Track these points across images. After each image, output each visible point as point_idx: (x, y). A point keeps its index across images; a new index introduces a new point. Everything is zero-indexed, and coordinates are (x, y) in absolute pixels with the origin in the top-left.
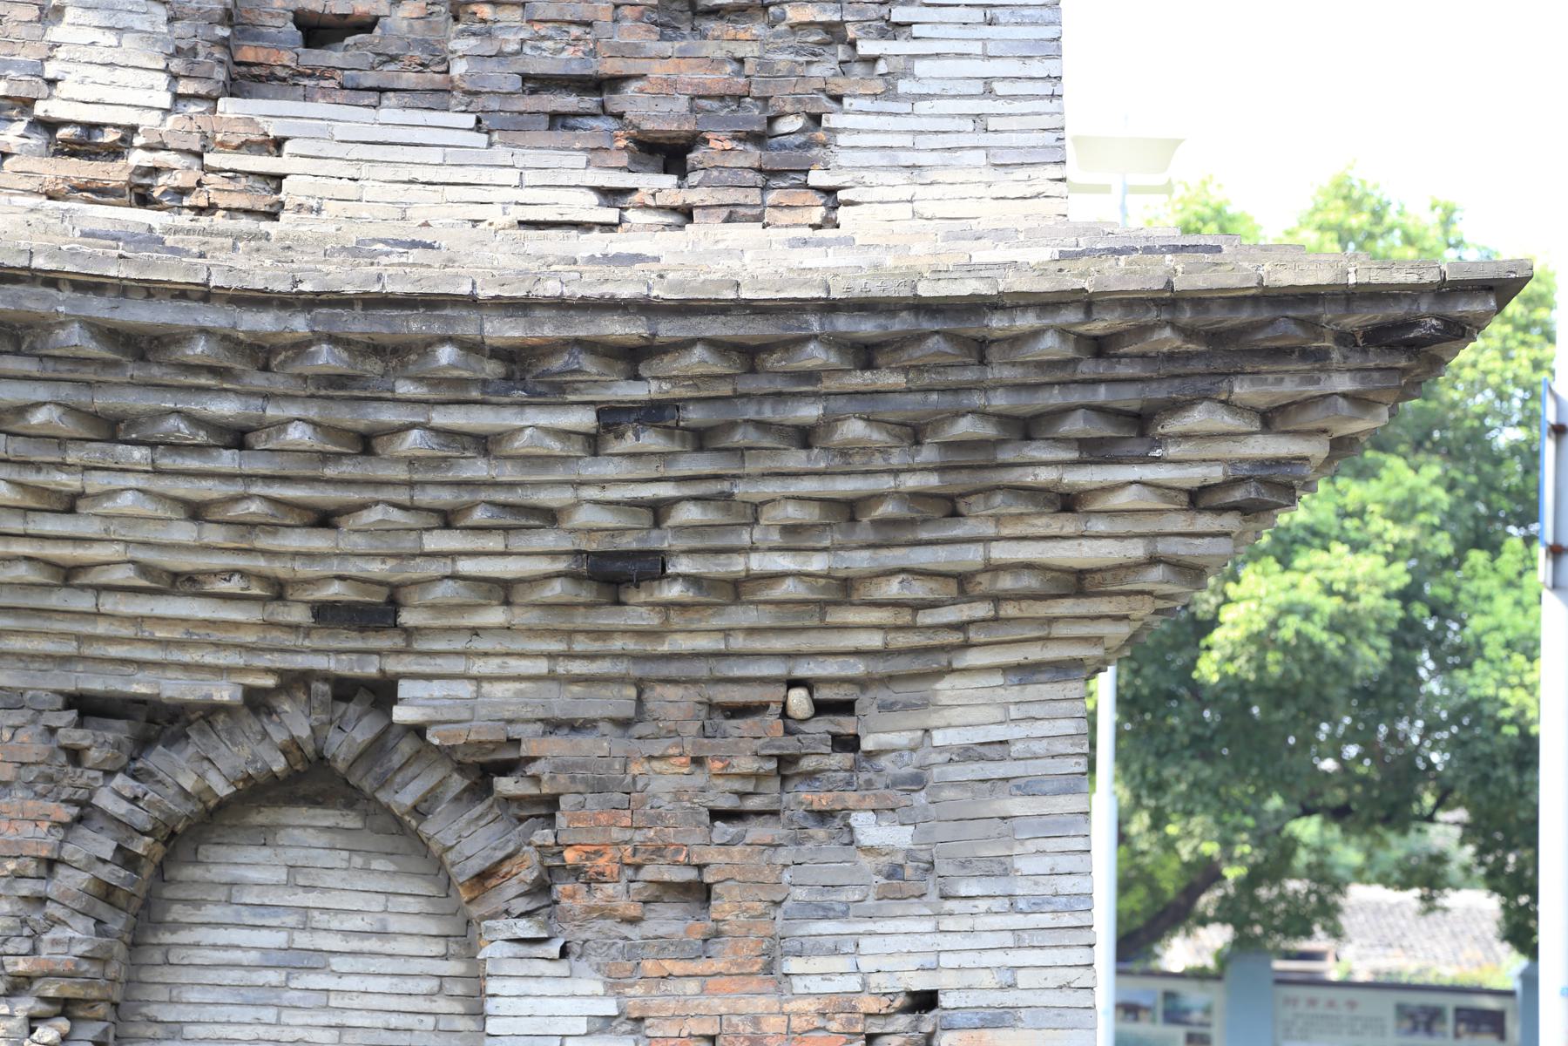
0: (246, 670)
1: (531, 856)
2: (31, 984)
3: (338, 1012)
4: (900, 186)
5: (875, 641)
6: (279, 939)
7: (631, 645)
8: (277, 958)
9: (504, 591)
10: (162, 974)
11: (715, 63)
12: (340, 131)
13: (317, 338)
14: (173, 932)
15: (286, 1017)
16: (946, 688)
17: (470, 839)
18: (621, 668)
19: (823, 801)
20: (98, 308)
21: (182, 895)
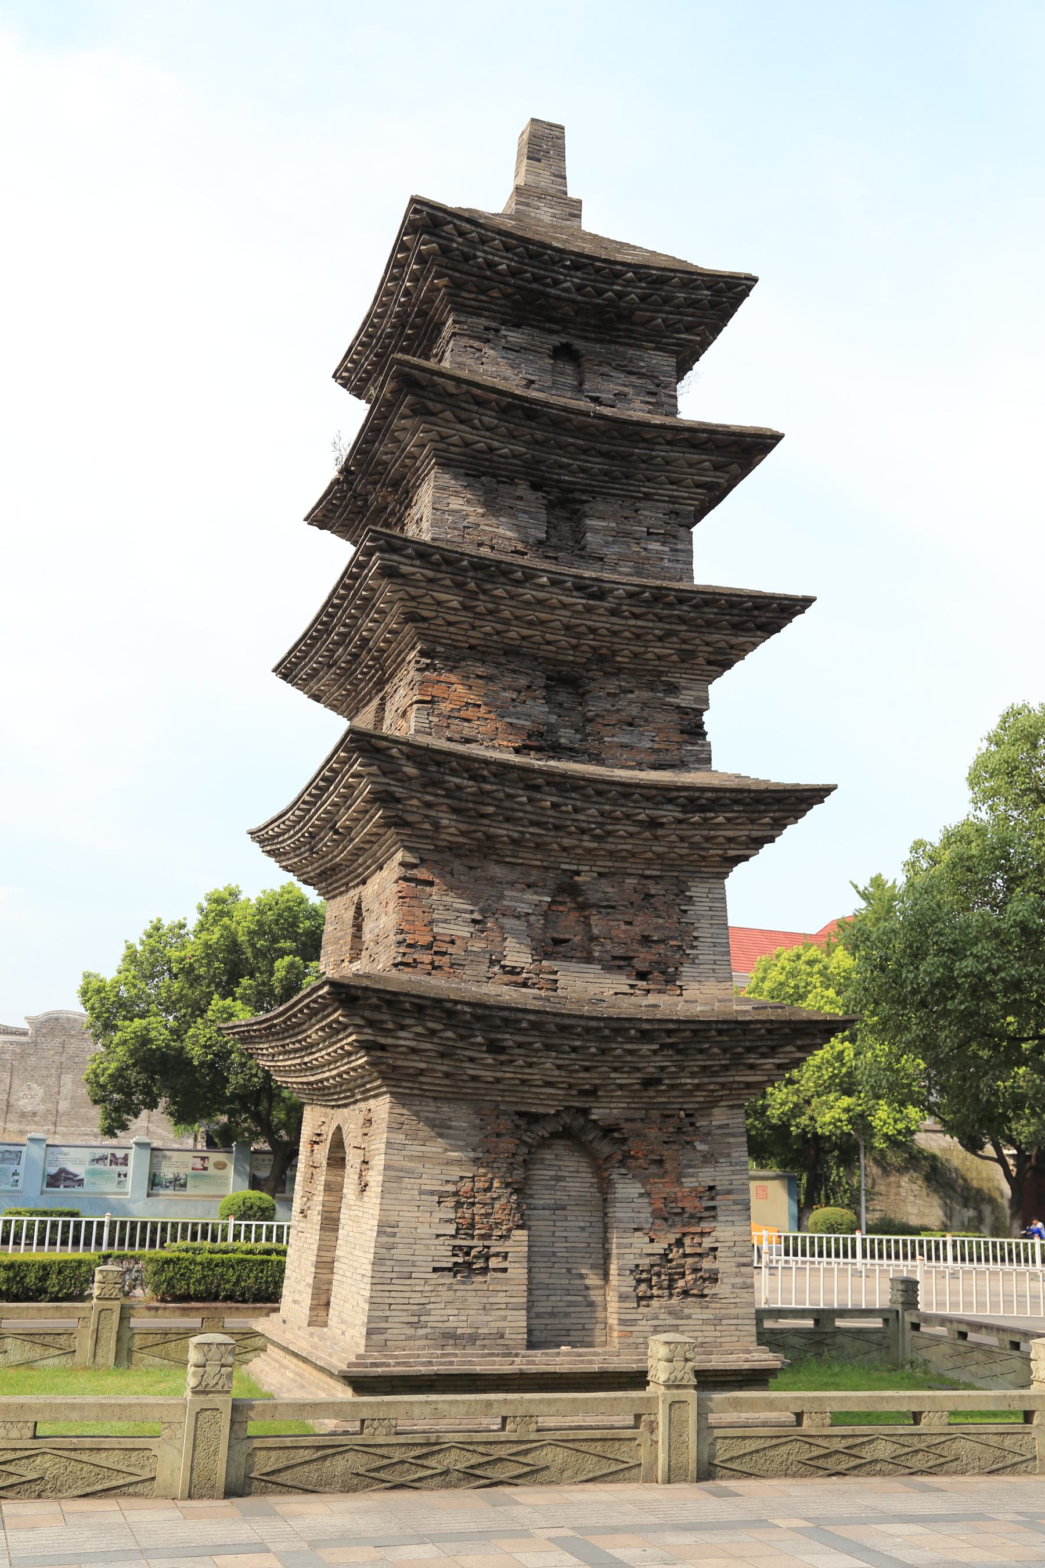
4: (696, 985)
5: (702, 1099)
6: (553, 1173)
9: (621, 1087)
11: (655, 954)
12: (571, 969)
13: (605, 1027)
16: (715, 1111)
17: (605, 1148)
18: (644, 1106)
19: (688, 1139)
20: (558, 1020)
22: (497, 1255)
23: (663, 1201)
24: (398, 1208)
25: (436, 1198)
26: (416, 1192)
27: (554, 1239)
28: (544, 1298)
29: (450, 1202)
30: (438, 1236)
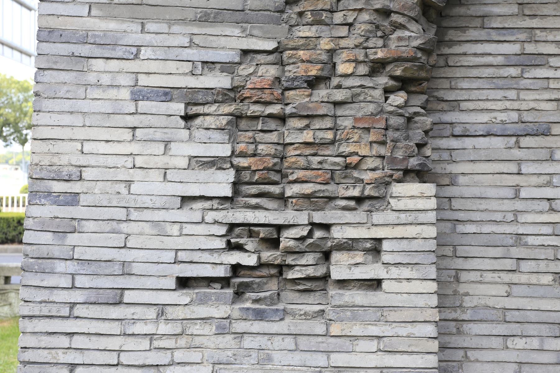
2: (384, 68)
3: (555, 91)
6: (515, 48)
8: (514, 60)
10: (444, 73)
14: (450, 47)
15: (523, 95)
21: (454, 24)
22: (348, 246)
24: (81, 134)
25: (179, 108)
26: (125, 94)
27: (519, 205)
28: (496, 342)
29: (216, 115)
30: (186, 200)
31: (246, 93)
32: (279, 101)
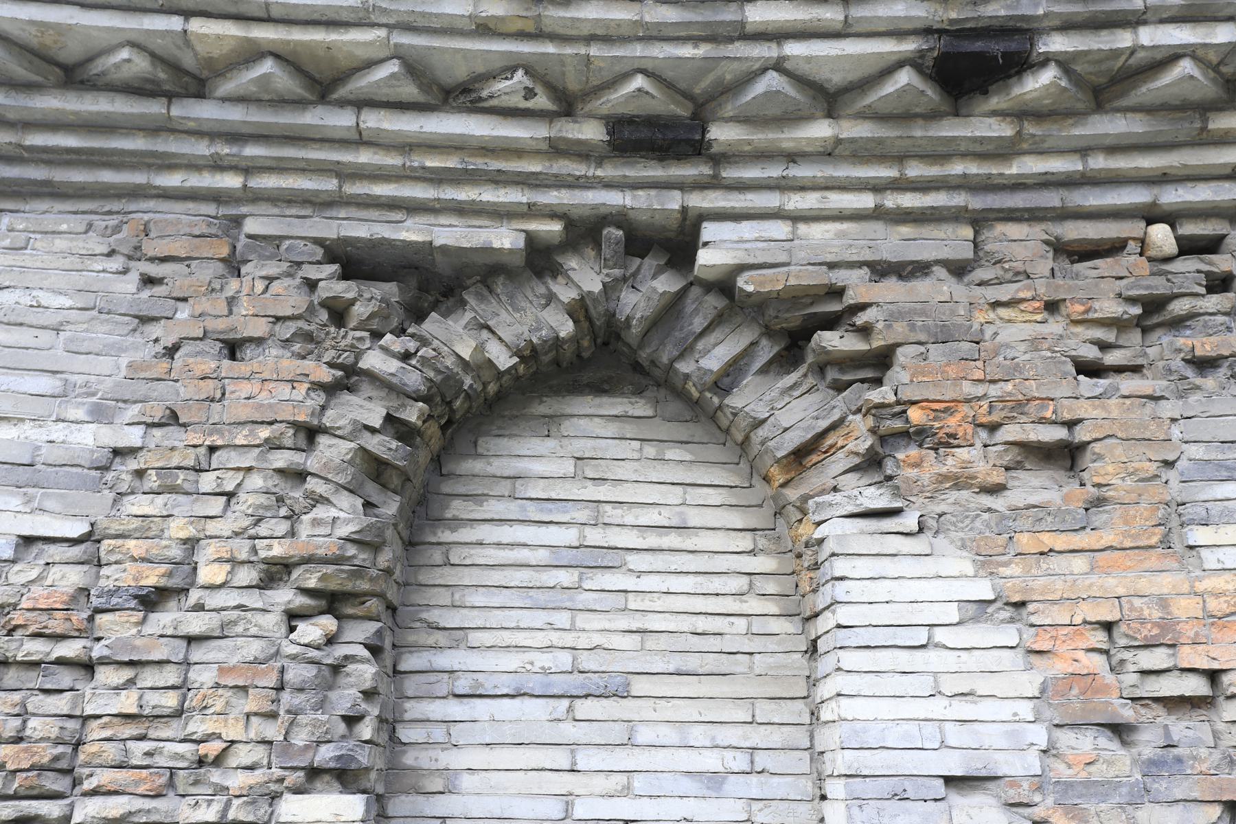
0: (531, 211)
1: (860, 424)
2: (290, 573)
3: (638, 615)
6: (568, 536)
7: (973, 168)
8: (567, 557)
10: (442, 576)
14: (453, 530)
15: (582, 620)
17: (786, 409)
18: (958, 199)
21: (462, 490)
23: (1098, 638)
31: (17, 618)
32: (81, 633)
